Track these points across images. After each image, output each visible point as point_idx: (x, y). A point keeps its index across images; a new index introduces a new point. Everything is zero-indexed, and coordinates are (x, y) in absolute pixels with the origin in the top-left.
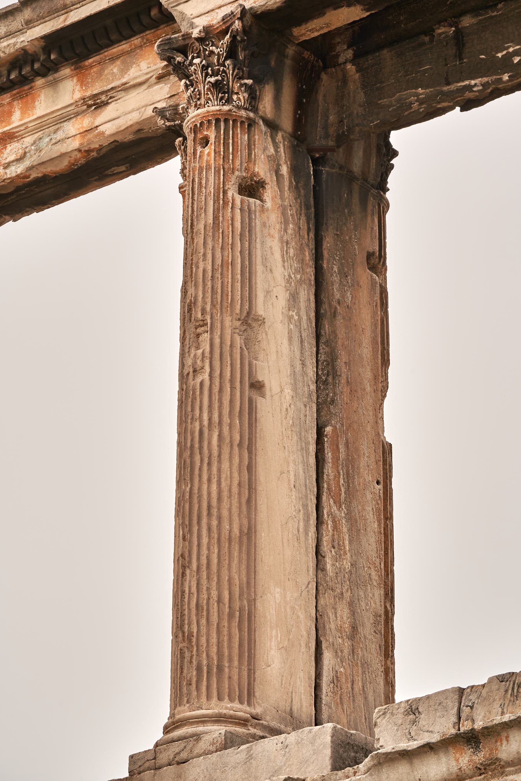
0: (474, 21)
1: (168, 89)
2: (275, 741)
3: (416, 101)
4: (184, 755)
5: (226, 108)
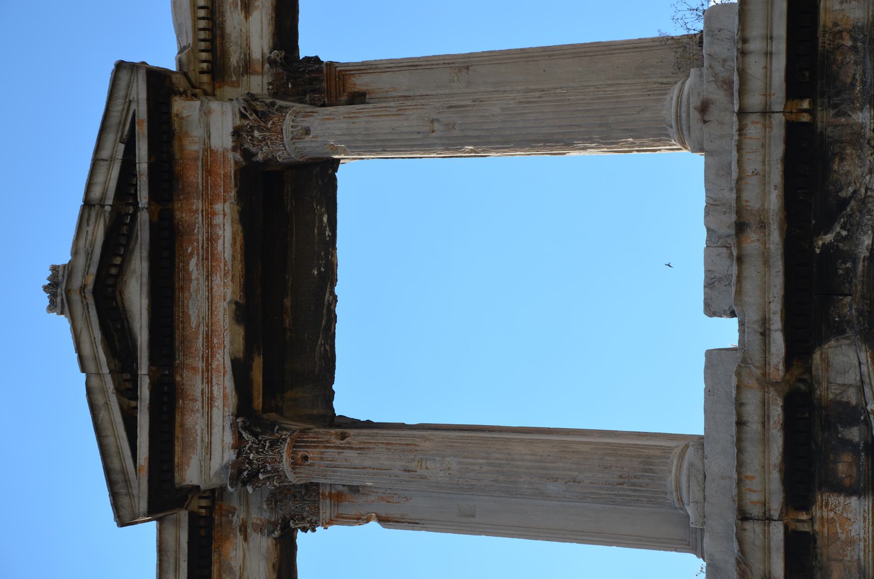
0: (289, 298)
1: (255, 534)
3: (324, 345)
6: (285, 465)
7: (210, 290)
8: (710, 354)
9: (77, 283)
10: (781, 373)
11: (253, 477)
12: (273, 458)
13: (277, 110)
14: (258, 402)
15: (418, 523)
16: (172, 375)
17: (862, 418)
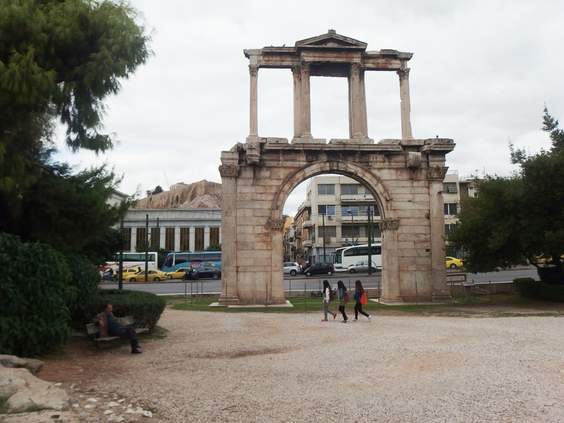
7: (332, 57)
8: (325, 140)
9: (333, 35)
11: (303, 64)
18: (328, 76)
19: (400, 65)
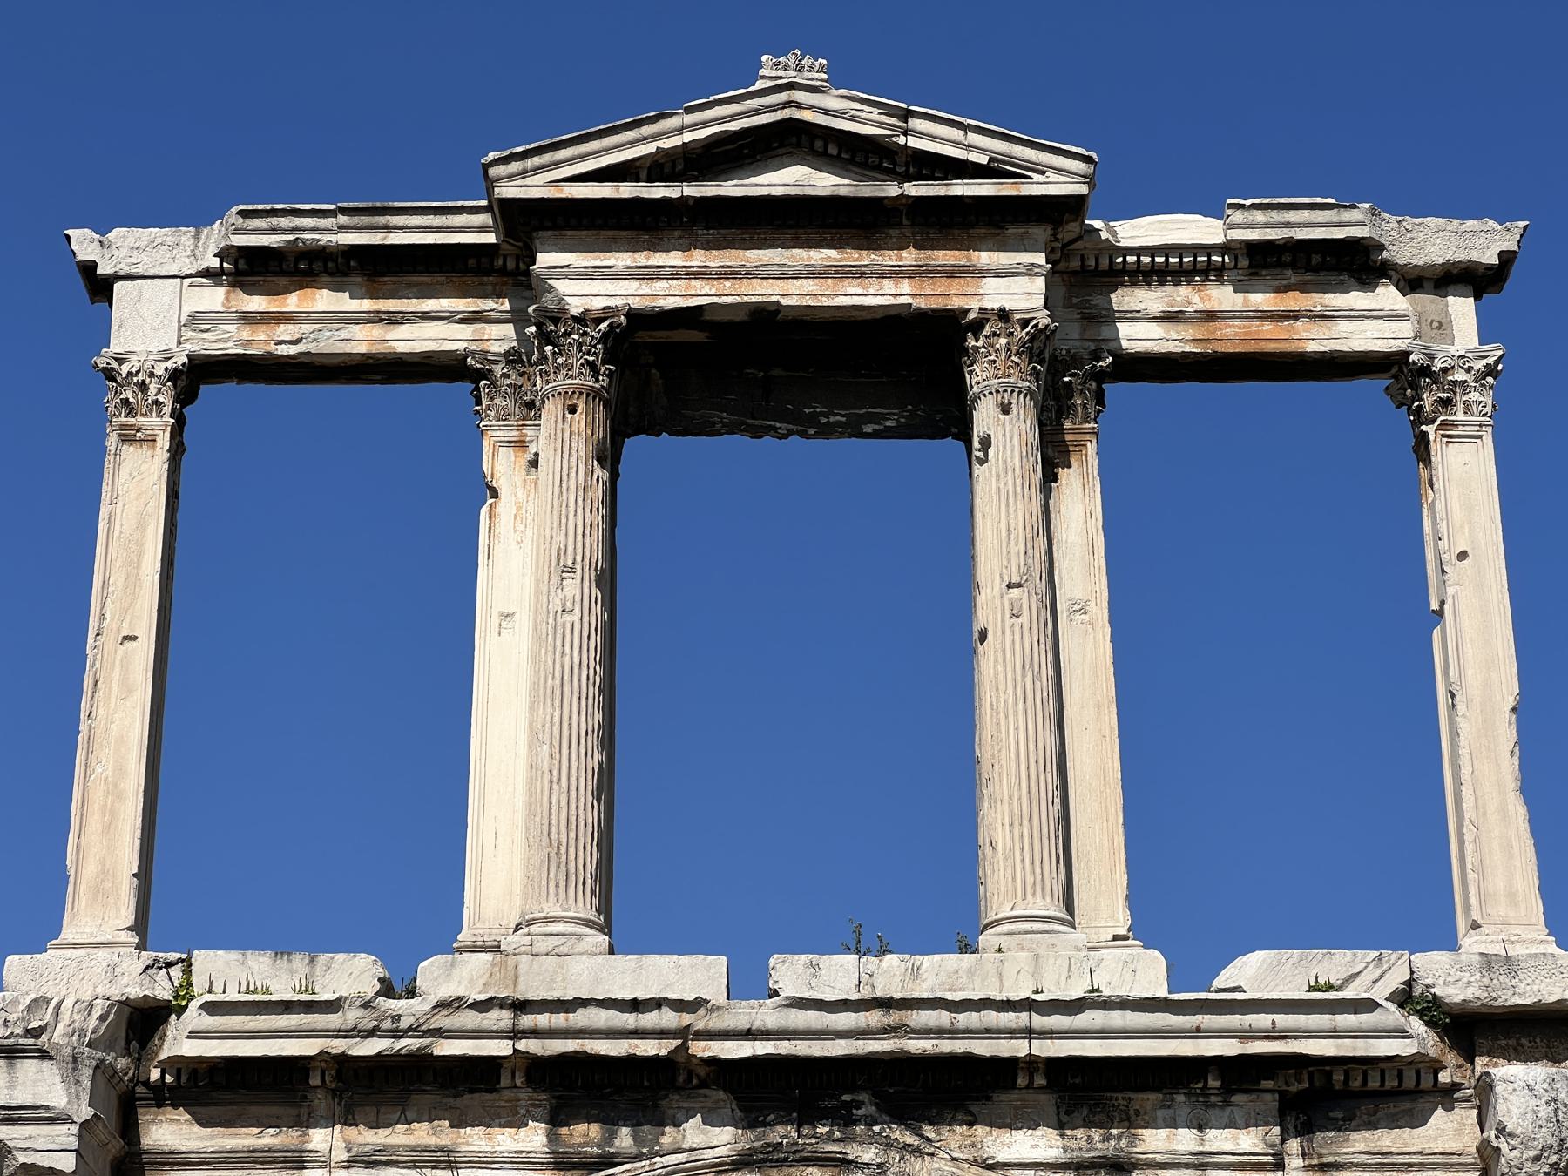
0: (783, 373)
2: (667, 960)
3: (721, 422)
4: (564, 950)
5: (597, 386)
6: (561, 381)
7: (796, 276)
10: (700, 1054)
11: (545, 337)
12: (572, 366)
13: (1034, 368)
14: (645, 337)
15: (488, 558)
16: (682, 226)
17: (645, 1151)
18: (785, 437)
19: (1406, 329)
